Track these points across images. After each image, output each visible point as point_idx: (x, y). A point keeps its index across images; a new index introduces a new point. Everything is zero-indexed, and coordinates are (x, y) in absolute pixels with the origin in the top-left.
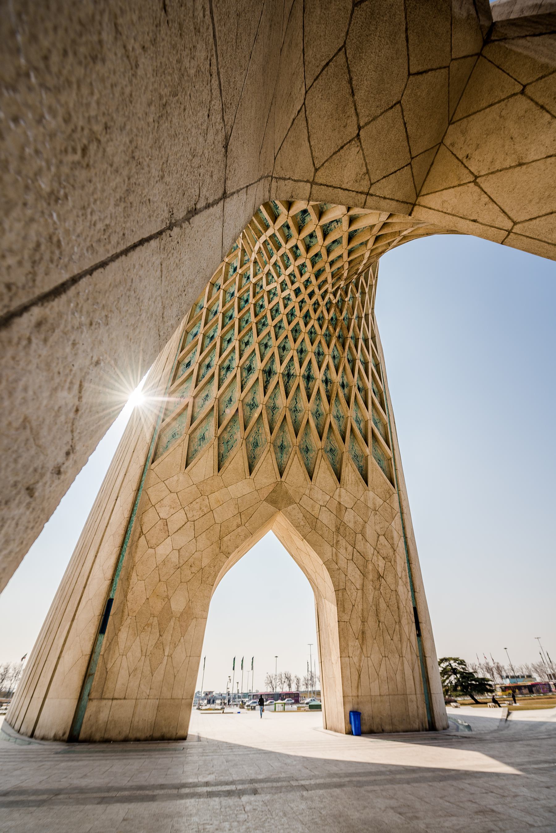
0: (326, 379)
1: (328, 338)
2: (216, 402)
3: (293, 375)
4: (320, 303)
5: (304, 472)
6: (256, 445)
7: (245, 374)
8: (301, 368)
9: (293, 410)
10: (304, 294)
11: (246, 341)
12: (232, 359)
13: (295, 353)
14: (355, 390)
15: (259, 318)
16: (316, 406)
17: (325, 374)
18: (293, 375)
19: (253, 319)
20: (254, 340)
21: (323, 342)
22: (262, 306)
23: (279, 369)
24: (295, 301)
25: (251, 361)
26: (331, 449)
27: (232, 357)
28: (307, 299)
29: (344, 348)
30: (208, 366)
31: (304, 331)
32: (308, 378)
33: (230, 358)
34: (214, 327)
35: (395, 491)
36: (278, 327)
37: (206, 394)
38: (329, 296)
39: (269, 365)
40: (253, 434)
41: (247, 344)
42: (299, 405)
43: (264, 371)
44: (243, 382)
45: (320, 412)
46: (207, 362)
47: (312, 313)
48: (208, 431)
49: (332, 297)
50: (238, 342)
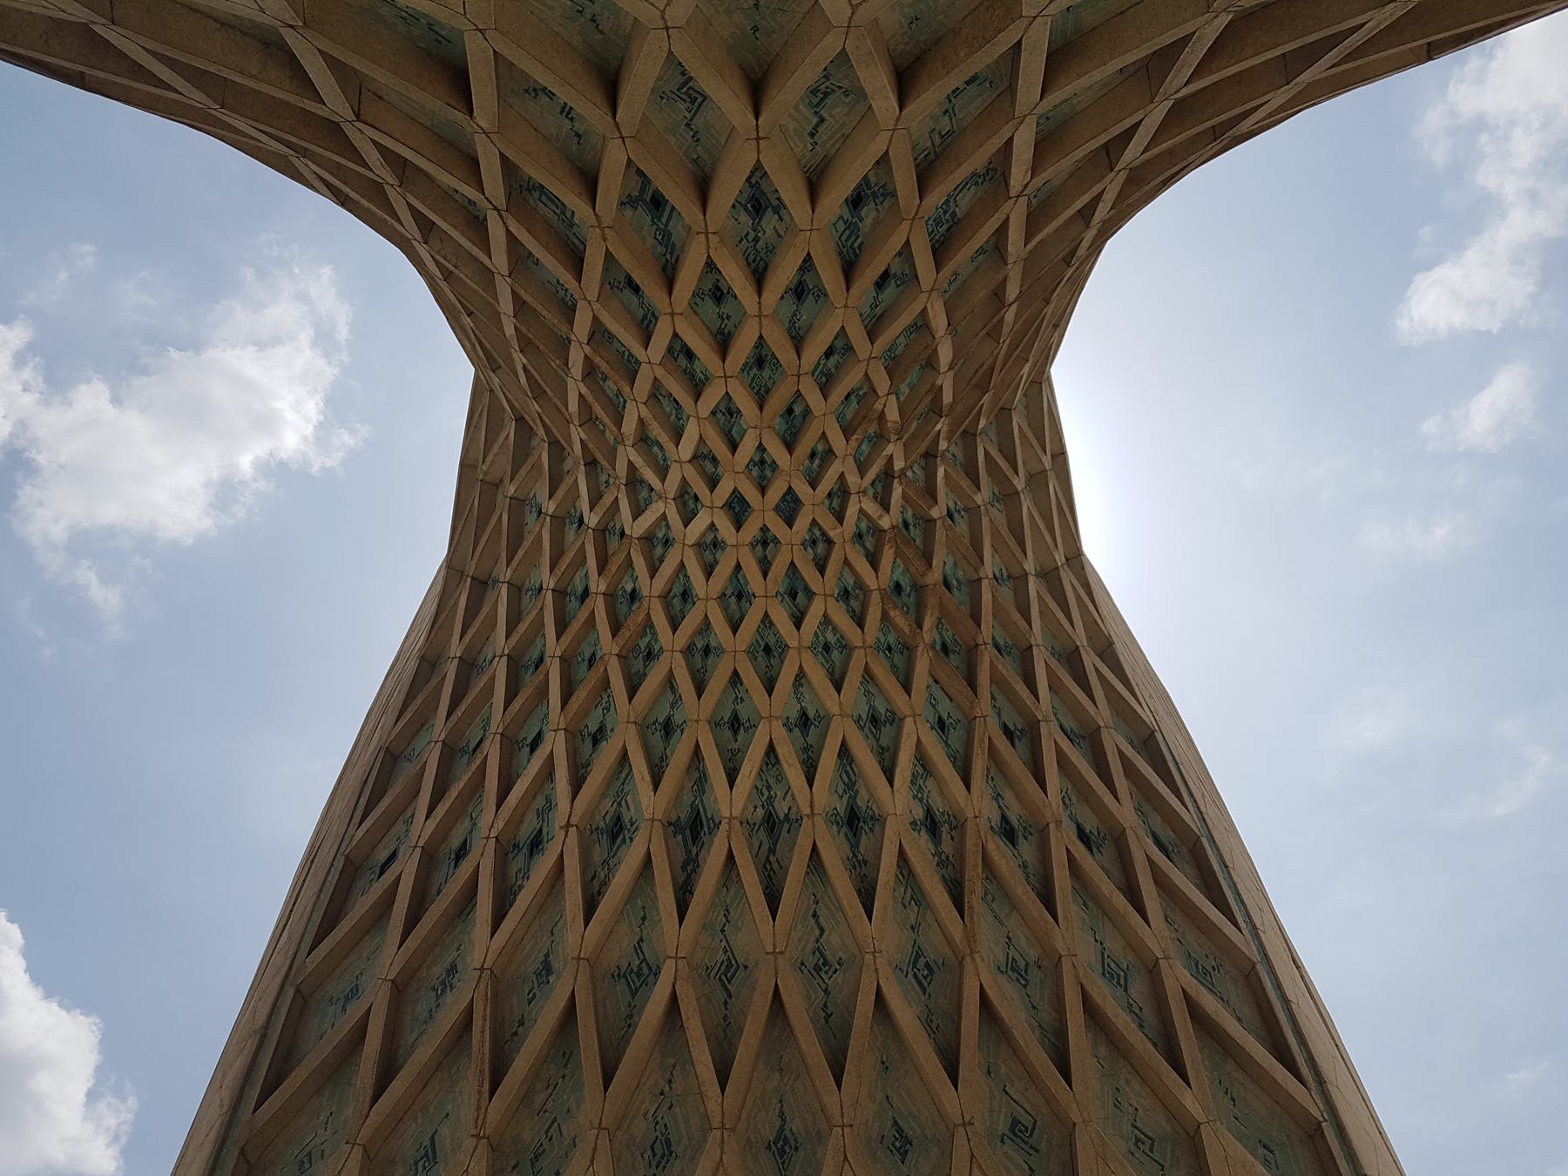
0: (929, 812)
1: (897, 658)
2: (482, 986)
4: (832, 534)
7: (599, 853)
8: (811, 786)
9: (810, 965)
10: (763, 512)
11: (593, 728)
12: (550, 805)
13: (780, 733)
14: (1063, 840)
15: (625, 633)
17: (919, 795)
18: (787, 817)
19: (608, 645)
20: (624, 713)
21: (881, 671)
22: (634, 596)
24: (737, 543)
26: (1015, 1123)
27: (548, 800)
28: (778, 528)
29: (972, 684)
30: (462, 852)
31: (793, 643)
32: (855, 821)
33: (540, 802)
34: (484, 713)
36: (701, 653)
37: (447, 964)
38: (861, 505)
39: (688, 798)
41: (598, 737)
43: (673, 826)
46: (455, 842)
47: (809, 573)
49: (871, 508)
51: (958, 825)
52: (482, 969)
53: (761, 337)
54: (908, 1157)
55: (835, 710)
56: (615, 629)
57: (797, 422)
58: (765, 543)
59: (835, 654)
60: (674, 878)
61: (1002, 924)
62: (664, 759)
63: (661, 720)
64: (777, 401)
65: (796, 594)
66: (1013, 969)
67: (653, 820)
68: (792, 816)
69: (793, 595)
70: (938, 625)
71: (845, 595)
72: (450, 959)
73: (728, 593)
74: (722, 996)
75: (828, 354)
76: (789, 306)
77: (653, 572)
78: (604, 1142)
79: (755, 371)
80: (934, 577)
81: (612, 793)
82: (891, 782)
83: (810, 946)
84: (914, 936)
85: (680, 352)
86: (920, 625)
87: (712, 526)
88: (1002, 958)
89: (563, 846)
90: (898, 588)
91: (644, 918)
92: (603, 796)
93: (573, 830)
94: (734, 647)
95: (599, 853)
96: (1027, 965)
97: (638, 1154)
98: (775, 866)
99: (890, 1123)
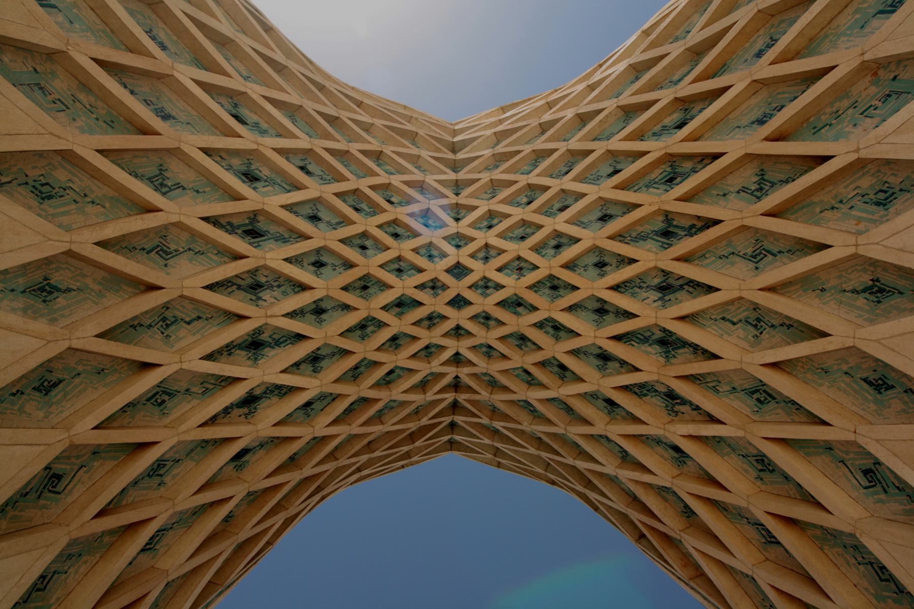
3: (259, 298)
6: (44, 194)
9: (168, 314)
10: (457, 287)
16: (184, 385)
18: (259, 298)
21: (351, 362)
23: (273, 256)
24: (437, 269)
25: (270, 182)
26: (59, 477)
32: (255, 345)
37: (167, 43)
39: (273, 229)
40: (80, 182)
42: (182, 333)
44: (219, 159)
45: (169, 404)
48: (67, 25)
52: (173, 68)
53: (578, 289)
54: (37, 394)
56: (372, 187)
58: (433, 288)
59: (359, 332)
60: (223, 216)
61: (188, 455)
62: (296, 213)
63: (320, 214)
66: (159, 465)
67: (264, 204)
68: (260, 302)
72: (169, 46)
73: (401, 263)
74: (148, 247)
79: (549, 284)
81: (273, 176)
83: (178, 313)
84: (182, 391)
85: (560, 242)
87: (444, 255)
88: (167, 457)
89: (247, 140)
91: (198, 192)
95: (236, 162)
96: (161, 475)
97: (44, 172)
98: (230, 290)
99: (61, 377)
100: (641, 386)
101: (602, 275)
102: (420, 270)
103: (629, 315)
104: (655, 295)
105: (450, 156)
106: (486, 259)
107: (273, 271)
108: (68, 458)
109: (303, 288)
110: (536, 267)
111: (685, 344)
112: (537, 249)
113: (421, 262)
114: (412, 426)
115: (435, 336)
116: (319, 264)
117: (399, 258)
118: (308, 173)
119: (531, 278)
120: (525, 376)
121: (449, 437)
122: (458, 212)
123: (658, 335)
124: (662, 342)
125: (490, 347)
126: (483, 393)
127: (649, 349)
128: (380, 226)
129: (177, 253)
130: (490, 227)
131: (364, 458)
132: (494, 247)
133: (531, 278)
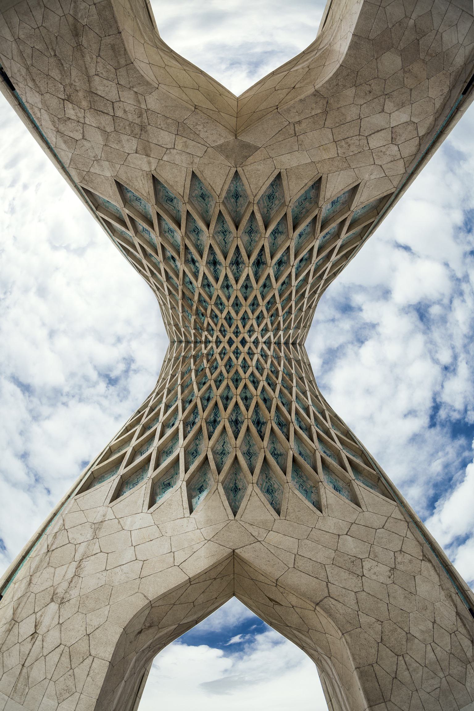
1: (203, 299)
5: (205, 179)
6: (270, 197)
9: (227, 233)
10: (237, 341)
11: (284, 285)
13: (235, 286)
17: (197, 268)
18: (233, 264)
21: (207, 299)
25: (278, 270)
29: (183, 293)
31: (230, 308)
32: (214, 263)
35: (79, 185)
39: (260, 270)
42: (220, 237)
45: (194, 233)
50: (293, 285)
51: (186, 261)
55: (219, 291)
56: (277, 309)
57: (228, 363)
58: (237, 332)
59: (219, 302)
62: (266, 279)
64: (233, 371)
65: (229, 319)
69: (230, 319)
70: (192, 305)
71: (216, 316)
74: (253, 227)
75: (220, 381)
76: (230, 395)
77: (266, 324)
78: (287, 203)
80: (193, 317)
82: (204, 273)
85: (255, 383)
86: (197, 307)
87: (250, 337)
88: (175, 233)
89: (294, 262)
90: (203, 315)
92: (283, 270)
93: (292, 265)
94: (245, 307)
95: (285, 258)
100: (197, 413)
101: (242, 399)
102: (244, 327)
103: (225, 409)
104: (234, 418)
105: (291, 341)
106: (249, 353)
107: (244, 270)
108: (178, 203)
109: (237, 281)
110: (245, 373)
111: (214, 429)
112: (252, 374)
113: (248, 327)
114: (181, 325)
115: (217, 333)
116: (246, 287)
117: (249, 319)
118: (282, 285)
119: (241, 371)
120: (201, 369)
121: (176, 340)
122: (268, 343)
123: (218, 420)
124: (215, 421)
125: (212, 355)
126: (194, 353)
127: (212, 416)
128: (262, 311)
129: (250, 236)
130: (262, 356)
131: (169, 306)
132: (253, 357)
133: (241, 371)
